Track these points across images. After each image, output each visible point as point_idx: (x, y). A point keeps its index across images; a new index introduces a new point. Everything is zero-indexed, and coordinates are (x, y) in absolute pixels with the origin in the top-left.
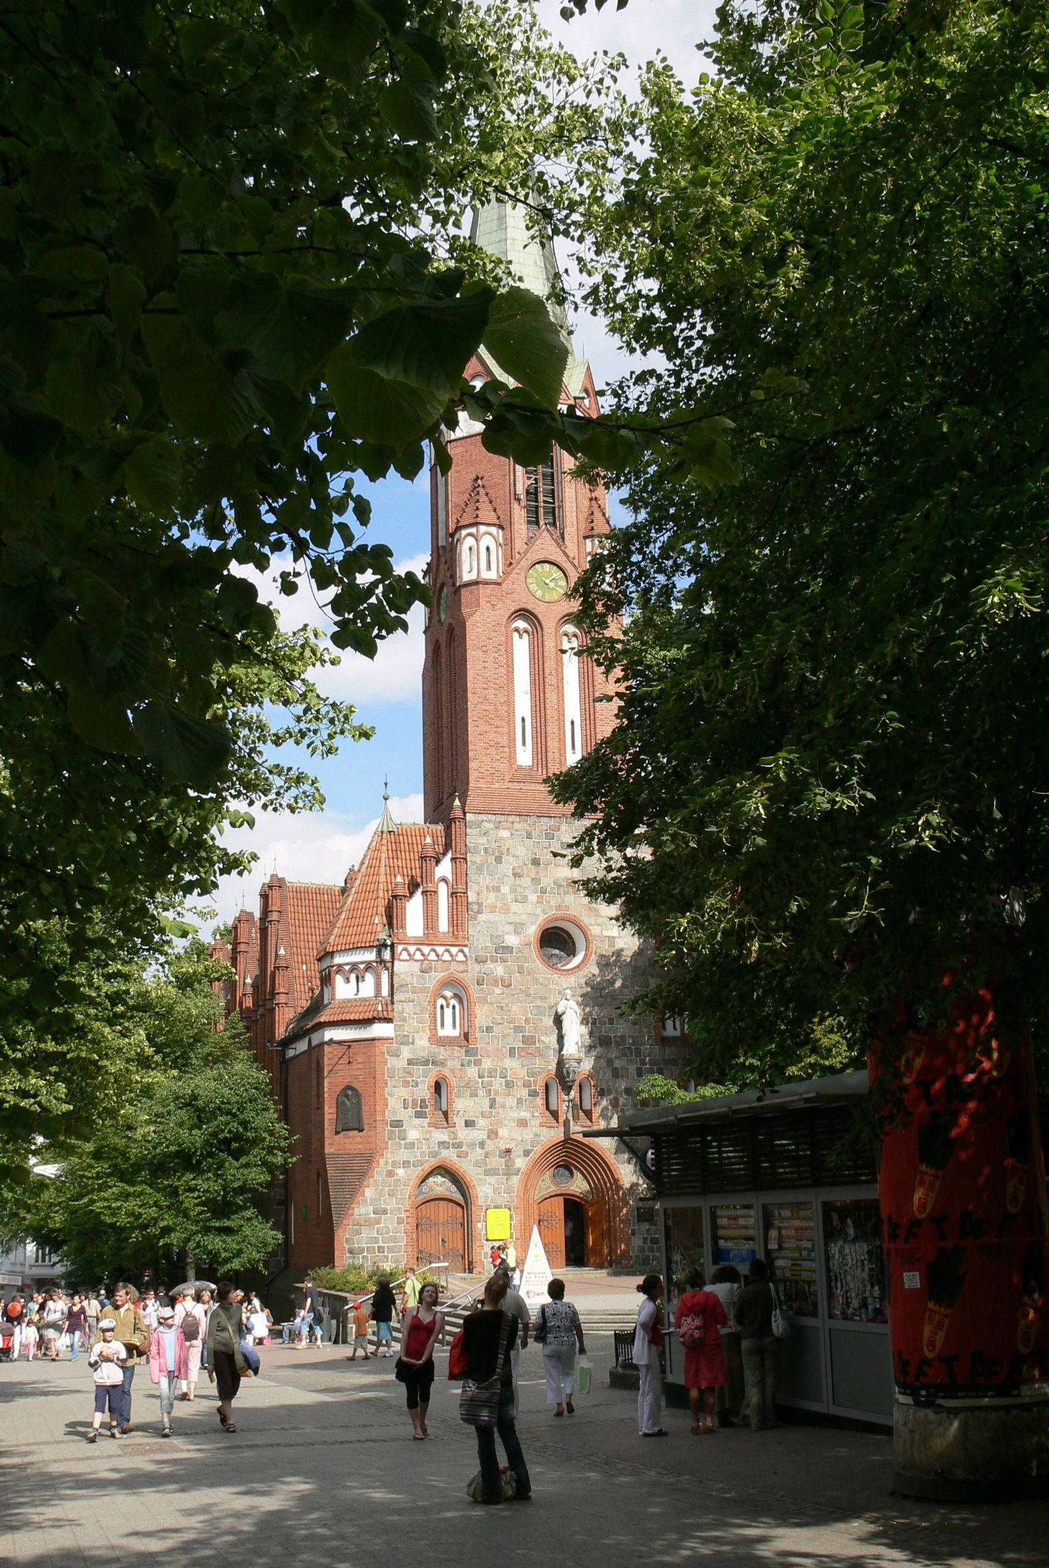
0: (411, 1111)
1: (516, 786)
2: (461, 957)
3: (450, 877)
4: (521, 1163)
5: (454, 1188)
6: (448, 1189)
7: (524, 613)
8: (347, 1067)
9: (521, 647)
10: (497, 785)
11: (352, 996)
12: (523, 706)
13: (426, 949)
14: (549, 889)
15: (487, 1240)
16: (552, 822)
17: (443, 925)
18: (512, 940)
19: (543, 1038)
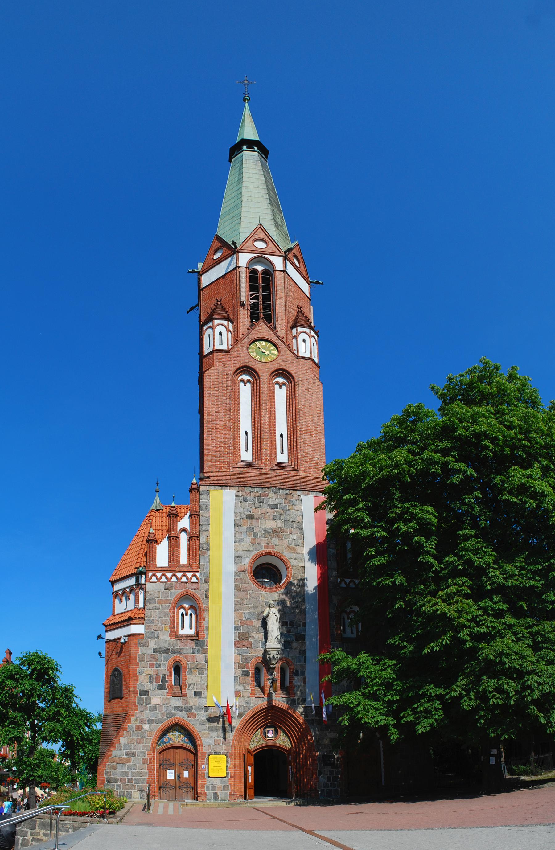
0: (155, 685)
2: (194, 580)
3: (188, 529)
5: (187, 740)
7: (247, 369)
10: (224, 470)
13: (169, 575)
14: (259, 534)
15: (209, 777)
16: (263, 491)
19: (253, 635)
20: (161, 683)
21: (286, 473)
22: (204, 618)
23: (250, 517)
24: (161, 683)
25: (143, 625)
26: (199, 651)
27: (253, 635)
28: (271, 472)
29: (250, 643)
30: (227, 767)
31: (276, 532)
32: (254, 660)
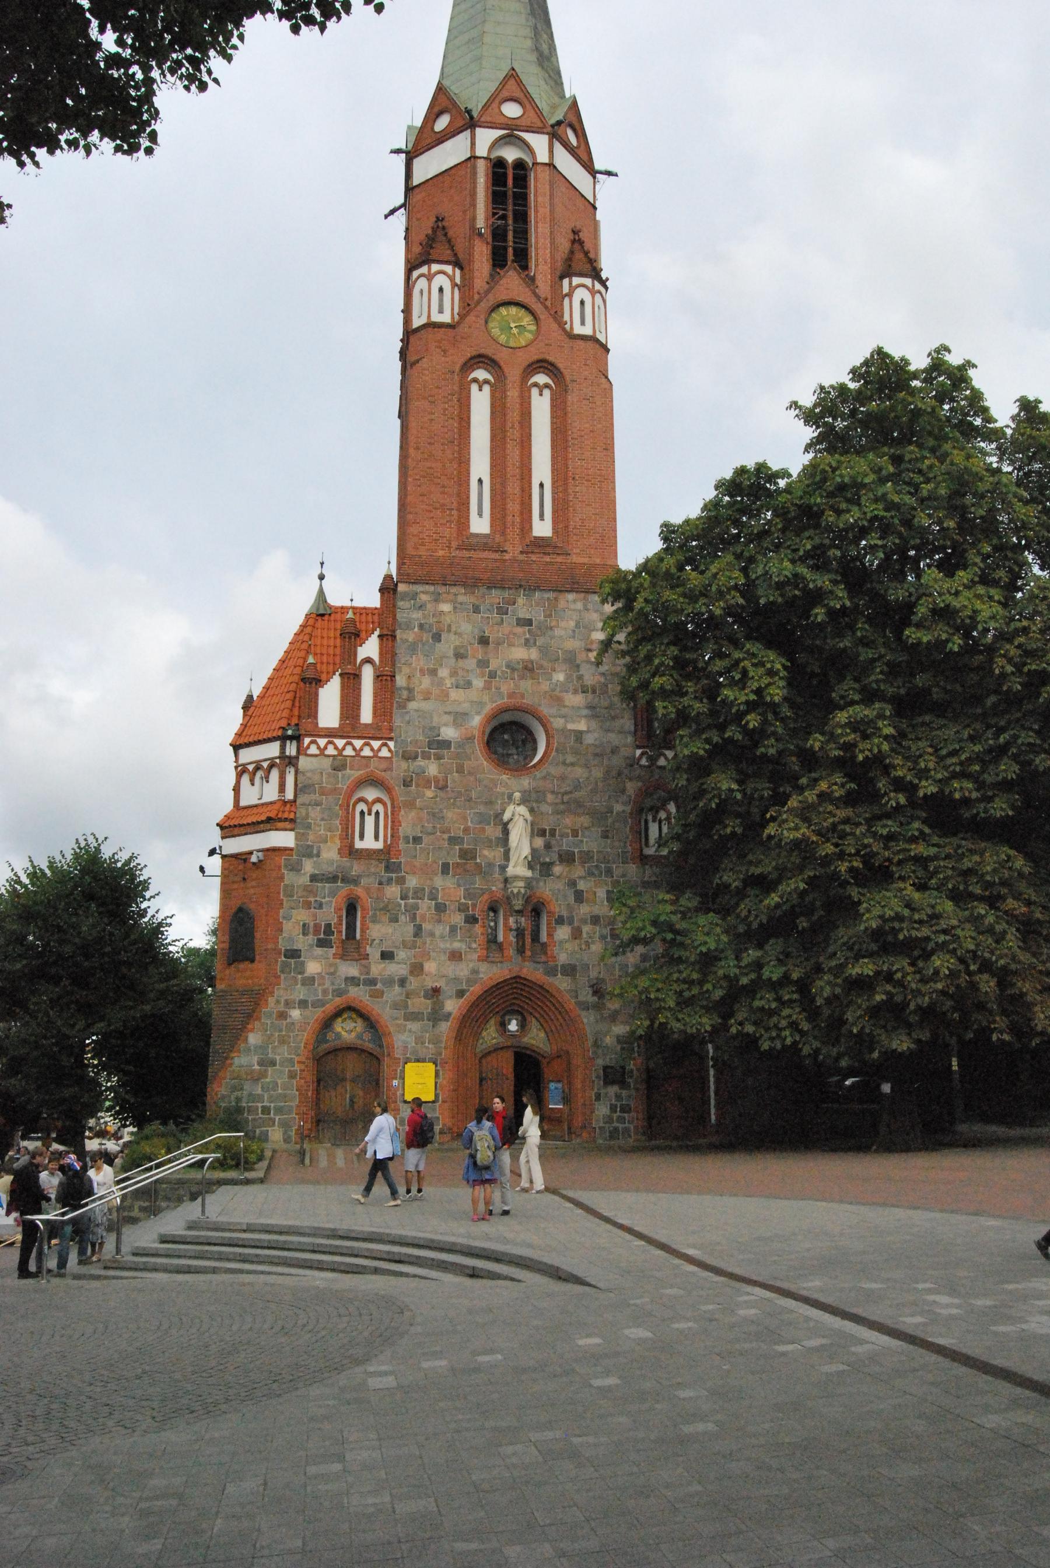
0: (311, 939)
1: (466, 554)
2: (384, 753)
3: (376, 658)
4: (452, 1006)
5: (367, 1036)
6: (359, 1037)
8: (242, 885)
9: (480, 402)
10: (441, 553)
11: (256, 802)
12: (480, 466)
13: (340, 743)
14: (499, 673)
16: (506, 594)
17: (366, 716)
18: (449, 733)
19: (486, 852)
20: (322, 936)
21: (547, 559)
22: (400, 822)
23: (484, 641)
24: (322, 936)
25: (292, 833)
26: (390, 880)
27: (486, 852)
28: (522, 557)
29: (479, 866)
30: (436, 1083)
31: (528, 669)
32: (486, 897)
